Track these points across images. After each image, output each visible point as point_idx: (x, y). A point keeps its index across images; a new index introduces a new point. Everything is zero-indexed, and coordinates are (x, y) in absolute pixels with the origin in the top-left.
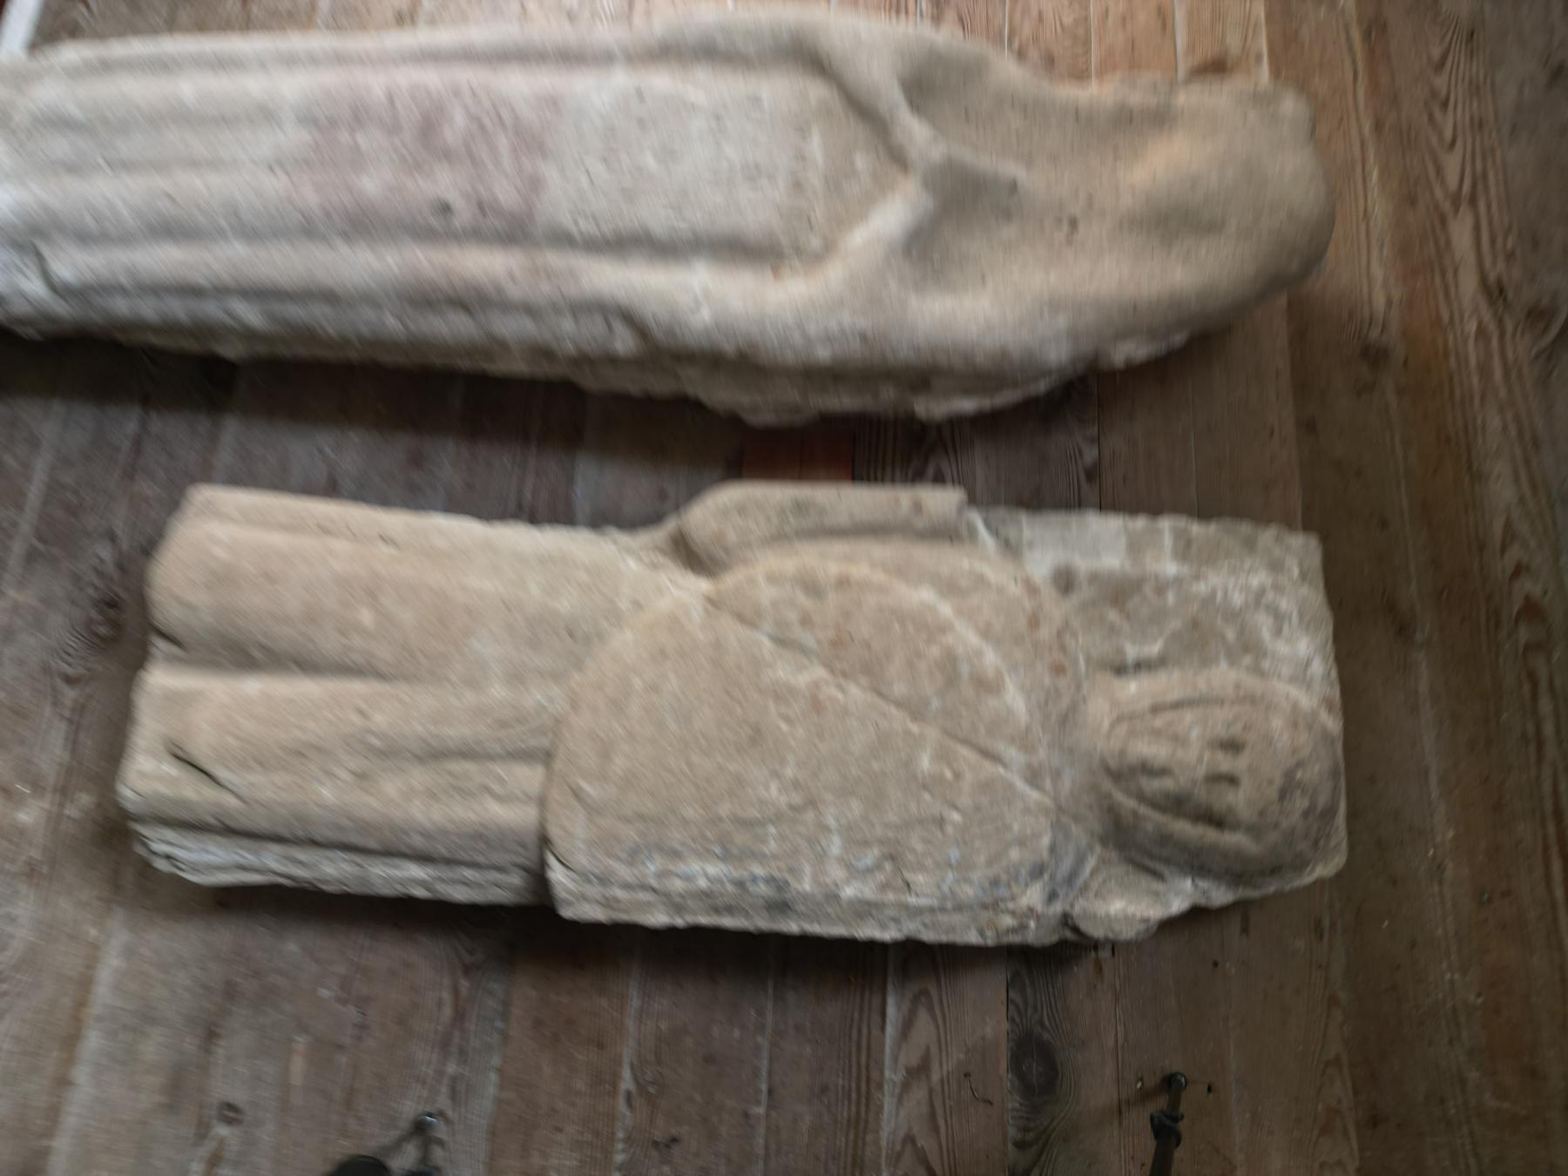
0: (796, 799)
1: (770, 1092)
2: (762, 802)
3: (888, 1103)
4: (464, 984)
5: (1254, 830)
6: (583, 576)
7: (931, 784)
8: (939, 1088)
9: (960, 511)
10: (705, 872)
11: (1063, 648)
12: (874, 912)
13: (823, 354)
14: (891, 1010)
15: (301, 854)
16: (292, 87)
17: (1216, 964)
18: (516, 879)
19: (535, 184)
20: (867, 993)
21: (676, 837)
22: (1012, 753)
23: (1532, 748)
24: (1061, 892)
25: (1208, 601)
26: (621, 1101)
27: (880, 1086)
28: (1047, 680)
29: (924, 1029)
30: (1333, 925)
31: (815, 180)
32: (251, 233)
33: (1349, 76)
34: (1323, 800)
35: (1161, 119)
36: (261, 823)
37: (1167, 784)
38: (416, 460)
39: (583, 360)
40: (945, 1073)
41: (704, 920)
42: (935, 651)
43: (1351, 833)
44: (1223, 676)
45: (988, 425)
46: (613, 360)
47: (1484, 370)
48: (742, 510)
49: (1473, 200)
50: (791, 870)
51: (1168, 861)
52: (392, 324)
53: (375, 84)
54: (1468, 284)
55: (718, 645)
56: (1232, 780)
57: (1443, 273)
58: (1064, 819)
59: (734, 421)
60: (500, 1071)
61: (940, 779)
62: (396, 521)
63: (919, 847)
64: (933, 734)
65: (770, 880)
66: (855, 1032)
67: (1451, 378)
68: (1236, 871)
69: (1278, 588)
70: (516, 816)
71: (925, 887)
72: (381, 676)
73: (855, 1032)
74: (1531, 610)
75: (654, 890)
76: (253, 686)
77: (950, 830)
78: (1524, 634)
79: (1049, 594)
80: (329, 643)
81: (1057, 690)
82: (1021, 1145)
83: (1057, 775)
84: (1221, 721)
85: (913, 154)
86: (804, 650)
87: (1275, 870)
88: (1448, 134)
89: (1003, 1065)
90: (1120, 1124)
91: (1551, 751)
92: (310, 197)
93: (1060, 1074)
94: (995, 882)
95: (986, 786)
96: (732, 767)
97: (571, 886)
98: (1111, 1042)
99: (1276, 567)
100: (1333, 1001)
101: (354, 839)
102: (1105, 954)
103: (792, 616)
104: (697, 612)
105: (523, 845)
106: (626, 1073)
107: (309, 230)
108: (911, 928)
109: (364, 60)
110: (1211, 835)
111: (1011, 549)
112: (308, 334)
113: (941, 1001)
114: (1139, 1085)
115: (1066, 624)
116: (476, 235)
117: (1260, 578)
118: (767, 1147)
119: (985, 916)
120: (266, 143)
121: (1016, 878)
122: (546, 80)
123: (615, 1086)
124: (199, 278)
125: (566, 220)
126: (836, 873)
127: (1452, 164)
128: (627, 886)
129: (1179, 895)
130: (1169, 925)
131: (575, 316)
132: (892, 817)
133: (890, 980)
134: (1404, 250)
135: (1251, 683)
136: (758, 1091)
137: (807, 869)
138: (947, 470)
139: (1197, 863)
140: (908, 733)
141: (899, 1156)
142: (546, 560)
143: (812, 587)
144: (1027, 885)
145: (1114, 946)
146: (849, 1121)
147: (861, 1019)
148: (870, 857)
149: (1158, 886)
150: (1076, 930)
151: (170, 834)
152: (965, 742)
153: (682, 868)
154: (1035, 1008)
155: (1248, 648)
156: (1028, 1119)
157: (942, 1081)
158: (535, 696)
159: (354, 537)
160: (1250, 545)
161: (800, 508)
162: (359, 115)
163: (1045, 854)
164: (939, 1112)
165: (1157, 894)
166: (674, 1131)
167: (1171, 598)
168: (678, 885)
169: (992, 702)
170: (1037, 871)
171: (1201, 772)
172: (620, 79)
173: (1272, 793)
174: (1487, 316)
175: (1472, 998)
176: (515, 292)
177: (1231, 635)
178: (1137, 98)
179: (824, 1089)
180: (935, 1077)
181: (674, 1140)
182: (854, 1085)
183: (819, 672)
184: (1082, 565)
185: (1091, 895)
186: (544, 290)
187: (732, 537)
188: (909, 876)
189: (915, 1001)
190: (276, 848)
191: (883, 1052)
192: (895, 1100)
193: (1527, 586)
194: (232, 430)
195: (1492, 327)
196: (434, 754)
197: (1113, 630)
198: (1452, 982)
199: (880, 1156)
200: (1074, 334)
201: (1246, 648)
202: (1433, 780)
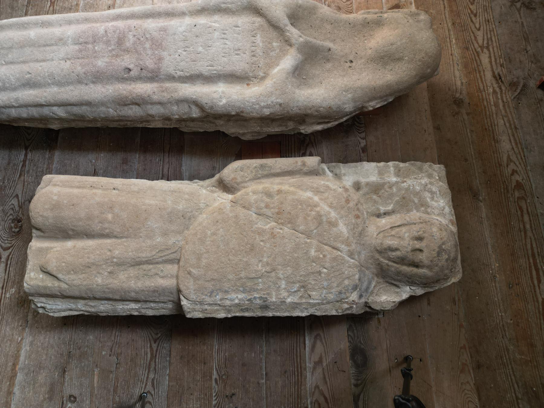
0: (268, 269)
1: (266, 374)
2: (256, 271)
3: (309, 375)
4: (154, 346)
5: (429, 267)
6: (187, 196)
7: (314, 260)
8: (326, 368)
9: (319, 165)
10: (237, 297)
11: (358, 209)
12: (298, 306)
13: (267, 112)
14: (307, 342)
15: (92, 303)
16: (71, 31)
18: (170, 306)
19: (160, 59)
20: (298, 337)
21: (226, 286)
22: (343, 247)
23: (523, 233)
24: (364, 294)
25: (407, 189)
26: (214, 382)
27: (305, 369)
28: (353, 221)
29: (319, 347)
30: (459, 300)
31: (259, 52)
32: (59, 84)
33: (442, 6)
34: (452, 255)
35: (379, 23)
36: (77, 293)
37: (398, 253)
38: (125, 162)
39: (181, 120)
40: (328, 362)
41: (237, 314)
42: (313, 213)
43: (463, 267)
44: (415, 215)
45: (326, 134)
46: (193, 120)
47: (496, 105)
48: (242, 170)
49: (488, 48)
50: (268, 294)
51: (400, 281)
52: (112, 112)
53: (101, 28)
54: (489, 75)
55: (236, 217)
56: (421, 251)
57: (480, 72)
58: (363, 268)
59: (237, 139)
60: (169, 375)
62: (118, 182)
63: (313, 283)
64: (315, 242)
65: (260, 298)
66: (295, 350)
67: (485, 108)
68: (425, 282)
69: (431, 183)
70: (169, 283)
71: (316, 296)
72: (116, 237)
73: (295, 350)
74: (519, 186)
75: (219, 305)
76: (70, 244)
77: (323, 275)
78: (517, 194)
79: (352, 191)
80: (97, 227)
81: (357, 225)
82: (356, 386)
83: (360, 253)
84: (415, 230)
85: (293, 41)
86: (268, 217)
87: (438, 281)
88: (478, 26)
89: (348, 358)
90: (391, 375)
91: (529, 234)
92: (79, 69)
94: (340, 293)
95: (335, 259)
96: (245, 259)
97: (189, 305)
98: (385, 347)
99: (430, 176)
100: (461, 326)
101: (111, 296)
102: (381, 316)
103: (263, 205)
104: (228, 206)
105: (172, 293)
106: (215, 372)
107: (79, 82)
108: (312, 311)
109: (96, 20)
110: (415, 270)
111: (338, 176)
112: (82, 118)
113: (325, 338)
114: (396, 361)
115: (359, 202)
116: (139, 79)
117: (425, 181)
118: (266, 394)
119: (338, 304)
120: (63, 51)
121: (347, 290)
122: (161, 23)
123: (211, 377)
124: (42, 101)
125: (171, 70)
126: (284, 294)
127: (480, 34)
128: (210, 305)
129: (405, 293)
130: (402, 304)
131: (177, 105)
132: (302, 273)
133: (306, 331)
134: (466, 66)
135: (424, 216)
136: (262, 374)
137: (274, 293)
138: (313, 151)
139: (411, 281)
140: (306, 243)
141: (314, 393)
142: (173, 192)
143: (269, 194)
144: (352, 293)
145: (384, 312)
146: (295, 382)
147: (297, 346)
148: (296, 287)
149: (398, 290)
150: (370, 307)
151: (43, 299)
152: (326, 244)
153: (229, 296)
154: (358, 338)
155: (423, 204)
156: (358, 376)
157: (327, 365)
158: (172, 240)
159: (102, 187)
160: (420, 169)
161: (262, 166)
162: (95, 39)
163: (357, 281)
164: (327, 376)
165: (397, 293)
166: (233, 391)
167: (395, 189)
168: (228, 303)
169: (335, 229)
170: (355, 288)
171: (410, 248)
172: (188, 21)
173: (435, 254)
174: (495, 86)
175: (509, 321)
176: (155, 98)
177: (416, 201)
178: (370, 17)
179: (285, 372)
180: (324, 364)
181: (233, 394)
182: (296, 370)
183: (273, 224)
184: (363, 180)
185: (375, 295)
186: (166, 96)
187: (239, 180)
188: (311, 293)
189: (316, 337)
190: (82, 302)
191: (306, 357)
192: (311, 373)
193: (517, 177)
194: (57, 154)
195: (498, 90)
196: (137, 263)
197: (375, 202)
198: (502, 315)
199: (307, 393)
200: (354, 100)
201: (422, 205)
202: (490, 247)
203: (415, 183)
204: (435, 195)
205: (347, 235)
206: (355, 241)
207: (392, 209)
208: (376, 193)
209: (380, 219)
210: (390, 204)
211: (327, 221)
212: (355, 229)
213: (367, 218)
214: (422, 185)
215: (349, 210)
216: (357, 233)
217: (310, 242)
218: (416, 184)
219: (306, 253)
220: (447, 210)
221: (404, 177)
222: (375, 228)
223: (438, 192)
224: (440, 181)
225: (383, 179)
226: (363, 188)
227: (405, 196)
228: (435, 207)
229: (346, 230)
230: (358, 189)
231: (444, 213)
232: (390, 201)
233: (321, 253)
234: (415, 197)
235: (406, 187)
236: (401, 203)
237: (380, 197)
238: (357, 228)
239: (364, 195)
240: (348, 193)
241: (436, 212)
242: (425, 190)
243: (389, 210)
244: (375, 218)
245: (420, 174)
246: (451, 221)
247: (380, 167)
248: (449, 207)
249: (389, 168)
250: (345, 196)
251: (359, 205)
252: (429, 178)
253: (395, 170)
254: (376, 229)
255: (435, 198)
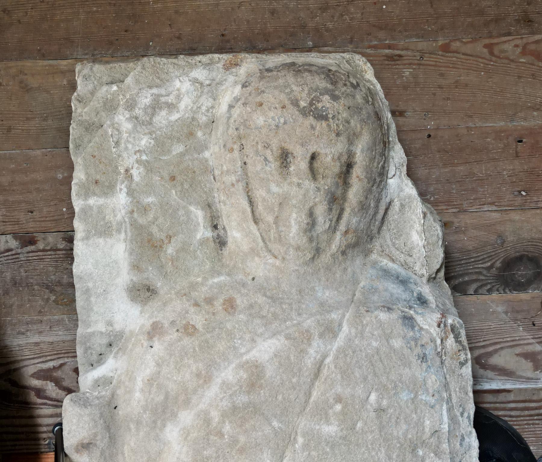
11: (209, 301)
17: (429, 136)
25: (148, 167)
28: (242, 316)
61: (343, 413)
69: (131, 105)
81: (251, 306)
93: (524, 253)
114: (524, 193)
152: (309, 394)
167: (150, 199)
169: (269, 372)
177: (178, 149)
197: (184, 249)
201: (191, 134)
203: (130, 146)
204: (163, 99)
205: (282, 339)
206: (294, 314)
207: (203, 209)
208: (161, 247)
209: (230, 240)
210: (188, 213)
211: (249, 393)
212: (264, 313)
213: (229, 275)
214: (135, 127)
215: (214, 329)
216: (272, 309)
217: (303, 436)
218: (133, 144)
219: (332, 447)
220: (200, 74)
221: (116, 170)
222: (256, 259)
223: (155, 91)
224: (123, 81)
225: (120, 224)
226: (147, 279)
227: (167, 178)
228: (194, 103)
229: (270, 341)
230: (148, 290)
231: (208, 82)
232: (181, 212)
233: (331, 408)
234: (169, 151)
235: (142, 169)
236: (186, 186)
237: (169, 237)
238: (261, 308)
239: (165, 276)
240: (166, 325)
241: (206, 102)
242: (150, 124)
243: (205, 218)
244: (226, 252)
245: (106, 132)
246: (228, 67)
247: (89, 232)
248: (192, 67)
249: (91, 208)
250: (175, 335)
251: (194, 294)
252: (115, 109)
253: (94, 194)
254: (258, 255)
255: (171, 99)
